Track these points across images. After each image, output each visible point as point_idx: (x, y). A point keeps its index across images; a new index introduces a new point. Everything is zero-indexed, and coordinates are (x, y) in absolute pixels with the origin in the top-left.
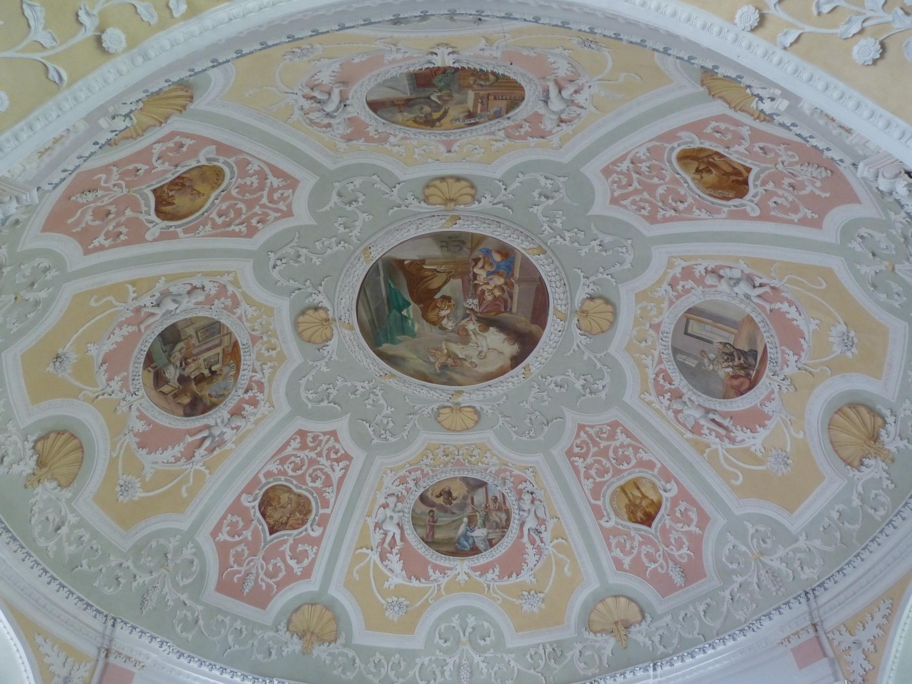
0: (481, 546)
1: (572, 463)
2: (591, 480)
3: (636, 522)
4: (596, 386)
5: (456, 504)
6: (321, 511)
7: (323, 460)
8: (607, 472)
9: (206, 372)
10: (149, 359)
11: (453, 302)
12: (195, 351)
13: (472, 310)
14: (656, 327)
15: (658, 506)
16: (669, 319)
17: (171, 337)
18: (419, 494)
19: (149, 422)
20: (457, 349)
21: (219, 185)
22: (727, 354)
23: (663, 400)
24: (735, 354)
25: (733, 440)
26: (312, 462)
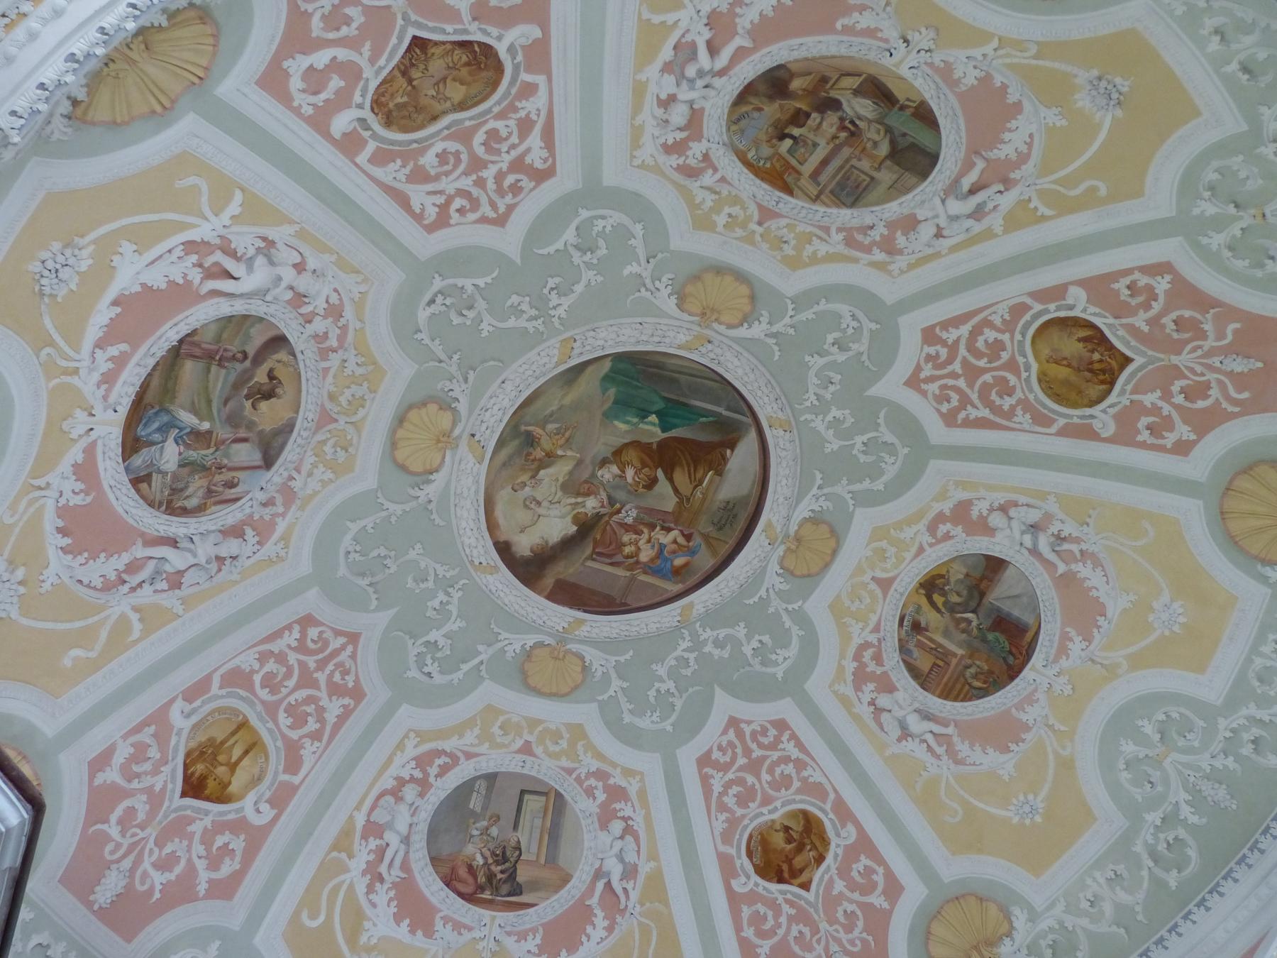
0: (138, 460)
1: (289, 627)
2: (256, 666)
4: (429, 661)
5: (242, 408)
6: (372, 146)
7: (467, 183)
8: (273, 691)
9: (796, 132)
10: (925, 116)
11: (641, 490)
12: (846, 152)
13: (619, 512)
14: (527, 749)
15: (222, 797)
16: (545, 769)
17: (915, 159)
18: (288, 336)
19: (847, 30)
20: (560, 470)
21: (1040, 381)
22: (504, 853)
23: (408, 767)
24: (507, 865)
25: (370, 889)
26: (477, 164)
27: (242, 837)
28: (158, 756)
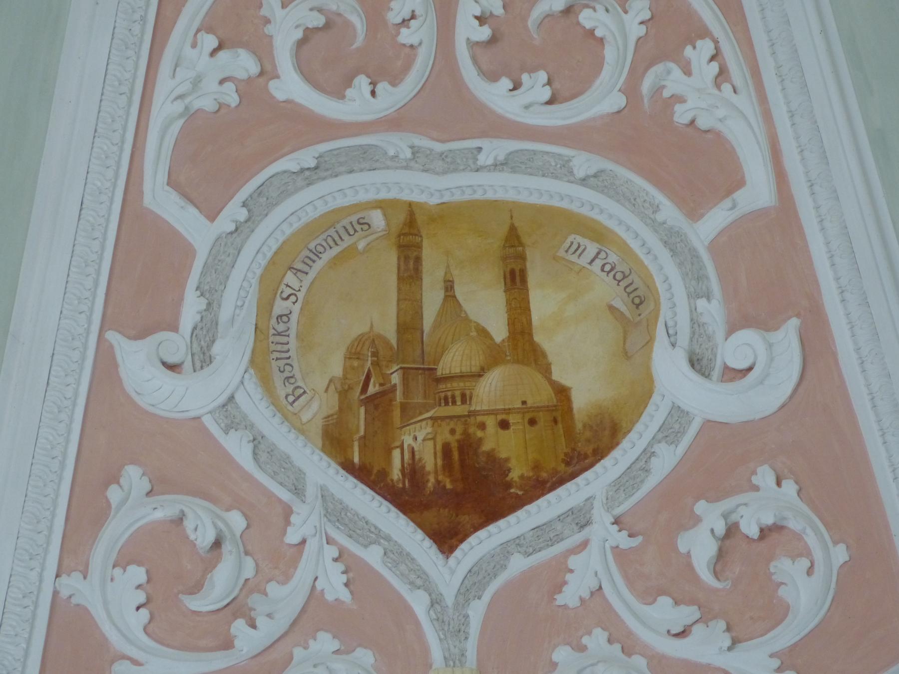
2: (244, 63)
3: (368, 475)
8: (385, 66)
15: (577, 443)
27: (765, 476)
28: (237, 521)
